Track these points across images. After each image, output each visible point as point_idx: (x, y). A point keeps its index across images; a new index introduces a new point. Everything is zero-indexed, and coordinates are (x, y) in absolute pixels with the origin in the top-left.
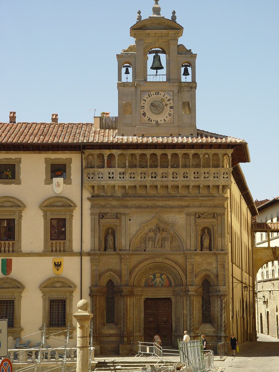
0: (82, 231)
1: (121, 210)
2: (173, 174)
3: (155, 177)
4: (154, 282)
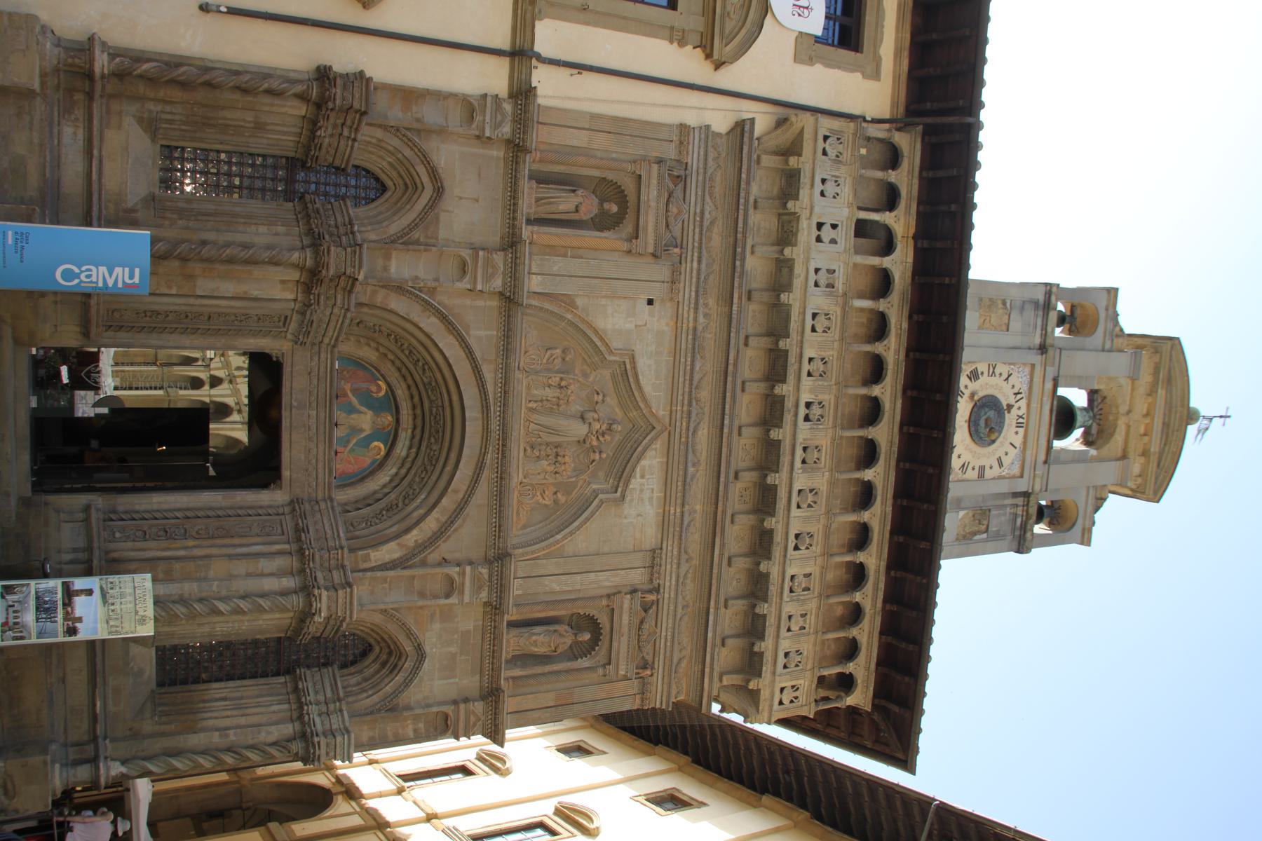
1: (691, 265)
2: (811, 491)
3: (807, 419)
4: (354, 401)
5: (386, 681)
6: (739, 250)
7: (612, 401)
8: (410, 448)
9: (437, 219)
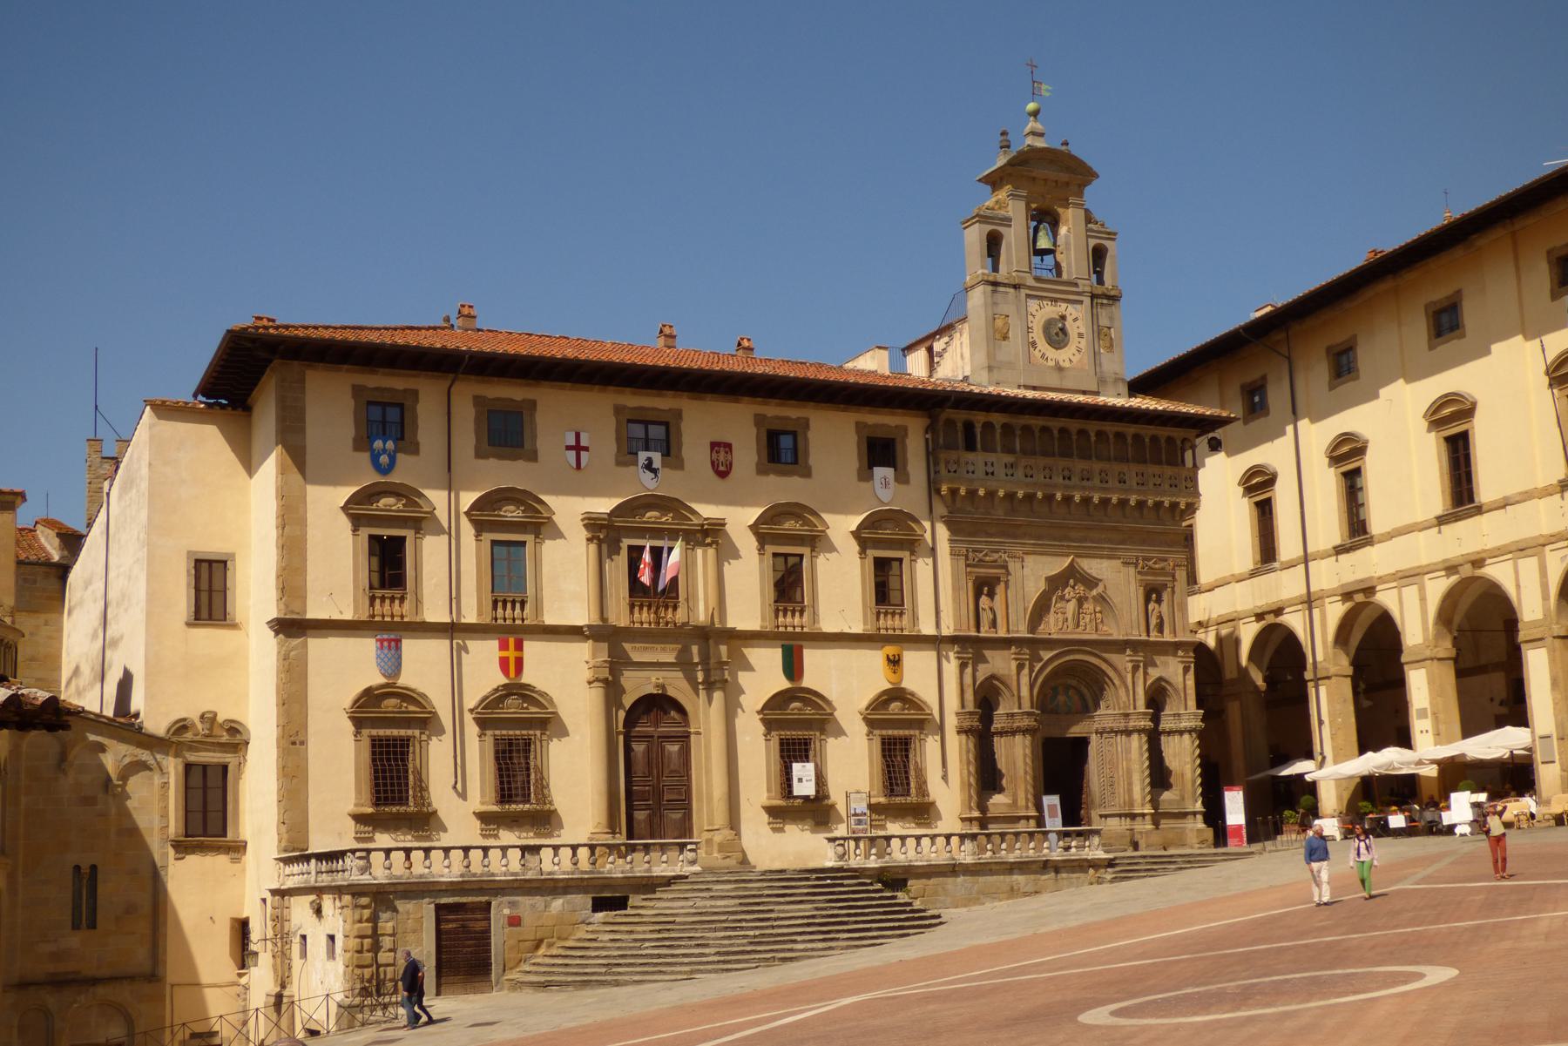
0: (935, 587)
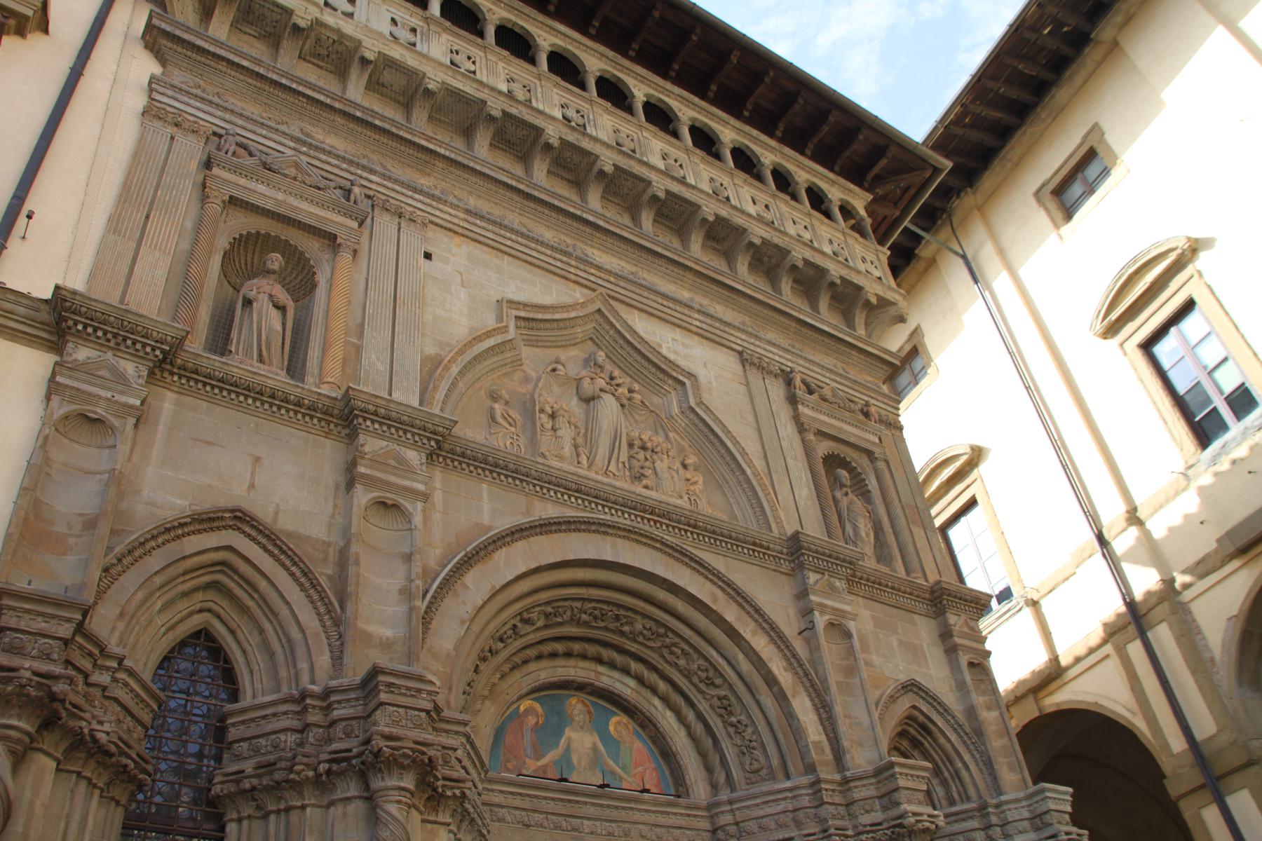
4: (551, 756)
5: (942, 740)
6: (358, 114)
7: (563, 355)
8: (626, 671)
9: (290, 535)
